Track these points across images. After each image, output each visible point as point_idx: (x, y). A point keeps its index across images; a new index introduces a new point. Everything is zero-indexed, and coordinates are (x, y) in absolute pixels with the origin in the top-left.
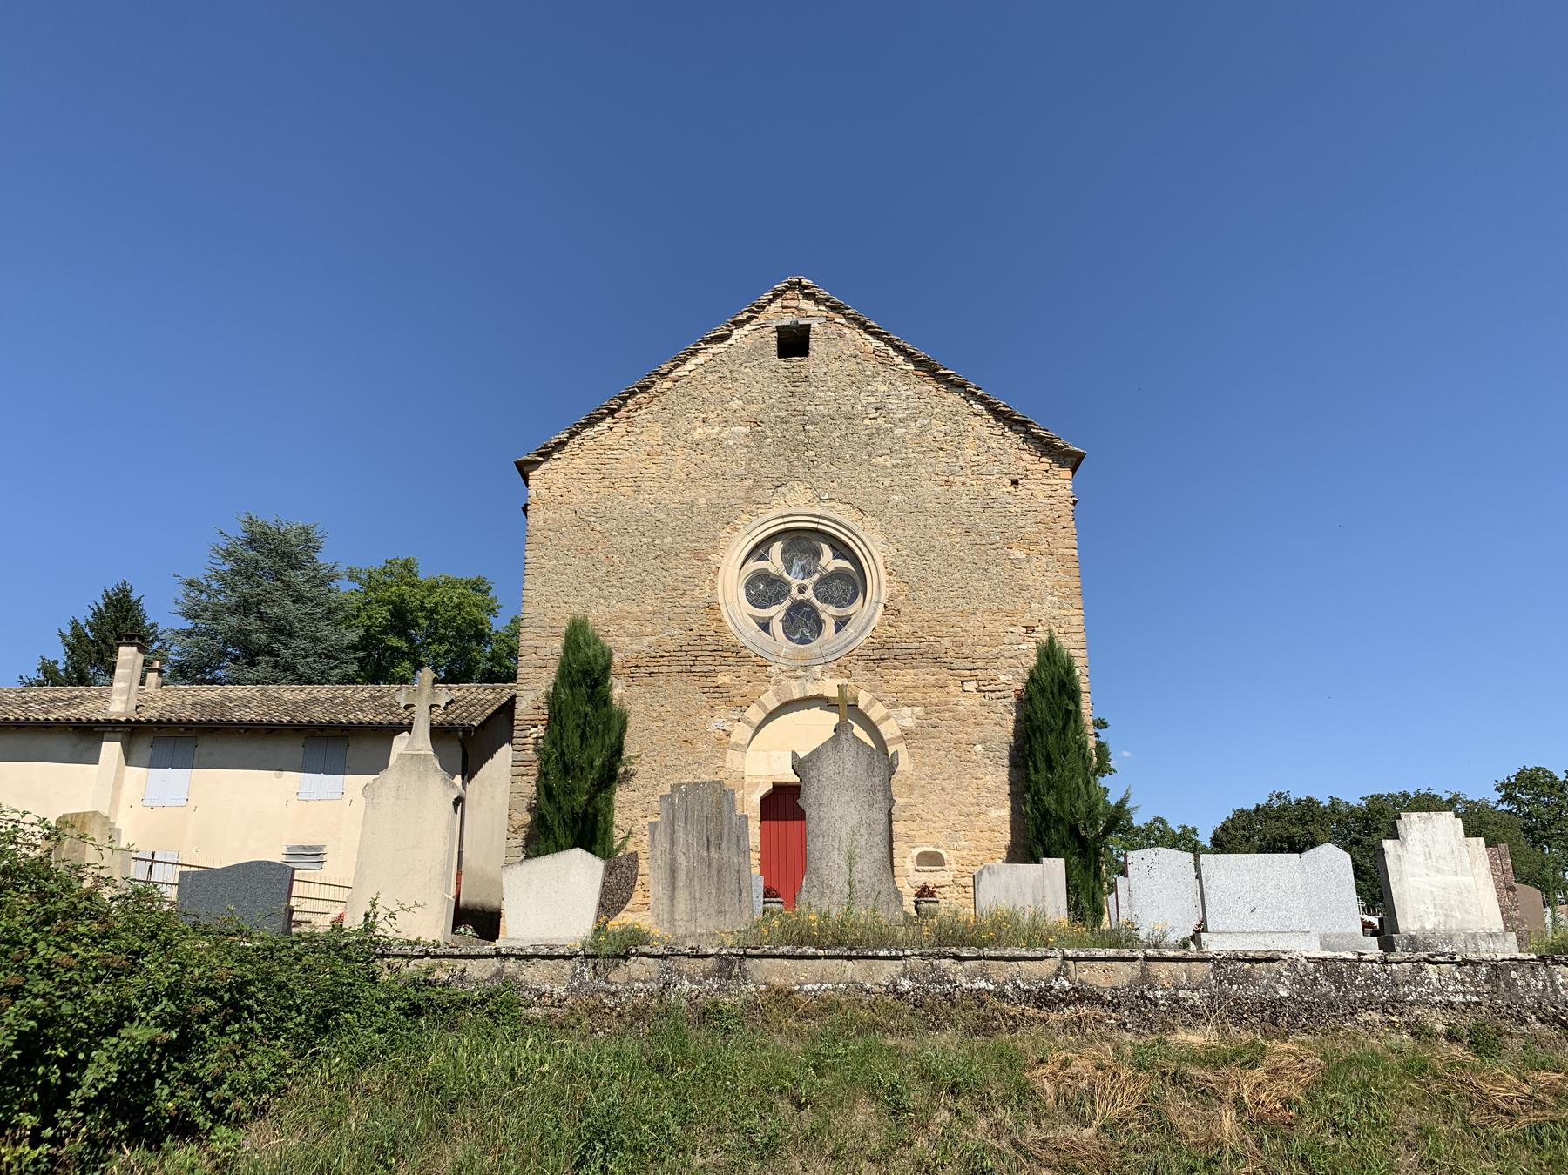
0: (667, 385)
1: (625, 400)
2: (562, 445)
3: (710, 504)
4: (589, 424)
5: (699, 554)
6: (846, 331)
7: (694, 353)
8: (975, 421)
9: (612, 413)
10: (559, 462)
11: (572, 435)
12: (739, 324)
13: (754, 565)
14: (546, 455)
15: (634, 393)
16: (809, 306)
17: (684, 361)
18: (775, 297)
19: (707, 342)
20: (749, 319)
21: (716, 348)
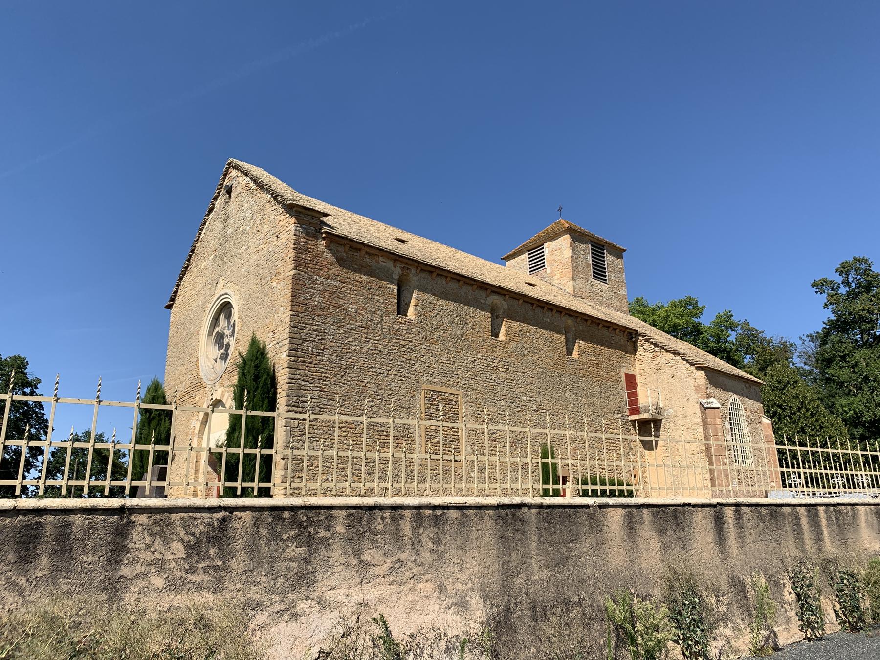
0: (199, 244)
1: (189, 260)
2: (176, 293)
3: (203, 304)
4: (181, 279)
5: (198, 331)
6: (240, 179)
7: (205, 224)
8: (268, 206)
9: (186, 268)
10: (178, 300)
11: (178, 285)
12: (215, 199)
13: (217, 329)
14: (173, 300)
15: (190, 256)
16: (234, 173)
17: (202, 230)
18: (225, 175)
19: (208, 215)
20: (219, 193)
21: (211, 216)
